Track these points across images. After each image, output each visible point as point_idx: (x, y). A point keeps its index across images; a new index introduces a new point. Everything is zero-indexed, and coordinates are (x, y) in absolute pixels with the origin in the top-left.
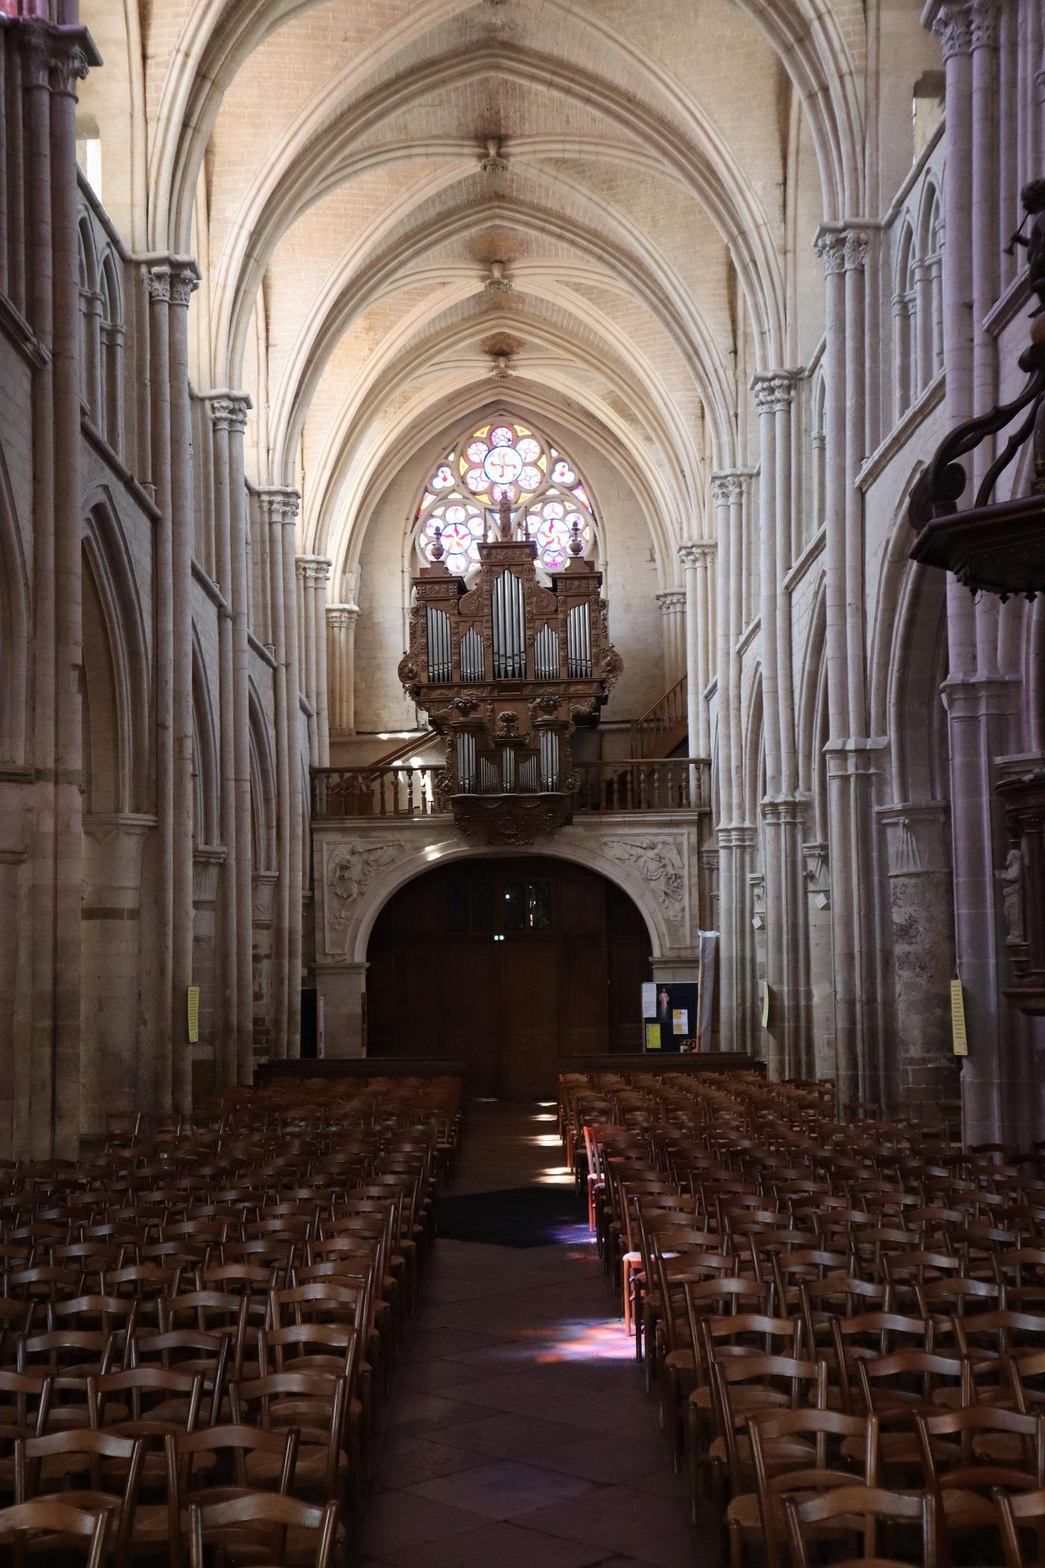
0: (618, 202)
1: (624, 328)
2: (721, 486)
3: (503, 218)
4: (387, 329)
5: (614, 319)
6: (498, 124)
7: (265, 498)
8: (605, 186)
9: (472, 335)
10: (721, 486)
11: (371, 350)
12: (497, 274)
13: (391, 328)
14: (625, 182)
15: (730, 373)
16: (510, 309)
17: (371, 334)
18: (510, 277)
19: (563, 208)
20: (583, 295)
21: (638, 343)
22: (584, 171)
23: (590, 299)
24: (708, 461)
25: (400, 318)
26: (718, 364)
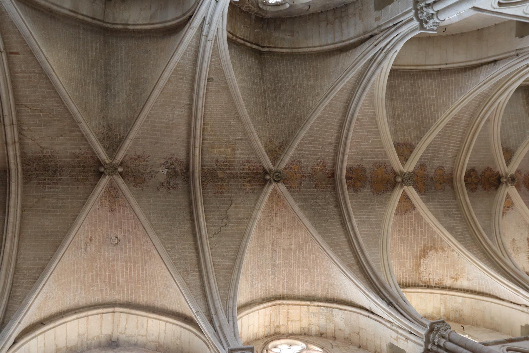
0: (307, 114)
1: (444, 112)
2: (426, 23)
3: (341, 175)
4: (442, 240)
5: (438, 118)
6: (256, 174)
7: (430, 347)
8: (300, 121)
9: (464, 195)
10: (426, 23)
11: (453, 250)
12: (399, 179)
13: (441, 238)
14: (299, 112)
15: (378, 36)
16: (452, 174)
17: (445, 248)
18: (402, 173)
19: (330, 144)
20: (424, 135)
21: (452, 104)
22: (292, 132)
23: (427, 132)
24: (518, 52)
25: (435, 232)
26: (372, 46)
